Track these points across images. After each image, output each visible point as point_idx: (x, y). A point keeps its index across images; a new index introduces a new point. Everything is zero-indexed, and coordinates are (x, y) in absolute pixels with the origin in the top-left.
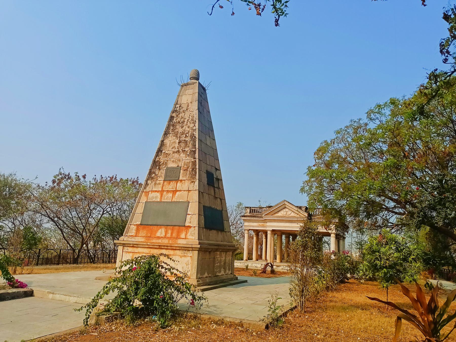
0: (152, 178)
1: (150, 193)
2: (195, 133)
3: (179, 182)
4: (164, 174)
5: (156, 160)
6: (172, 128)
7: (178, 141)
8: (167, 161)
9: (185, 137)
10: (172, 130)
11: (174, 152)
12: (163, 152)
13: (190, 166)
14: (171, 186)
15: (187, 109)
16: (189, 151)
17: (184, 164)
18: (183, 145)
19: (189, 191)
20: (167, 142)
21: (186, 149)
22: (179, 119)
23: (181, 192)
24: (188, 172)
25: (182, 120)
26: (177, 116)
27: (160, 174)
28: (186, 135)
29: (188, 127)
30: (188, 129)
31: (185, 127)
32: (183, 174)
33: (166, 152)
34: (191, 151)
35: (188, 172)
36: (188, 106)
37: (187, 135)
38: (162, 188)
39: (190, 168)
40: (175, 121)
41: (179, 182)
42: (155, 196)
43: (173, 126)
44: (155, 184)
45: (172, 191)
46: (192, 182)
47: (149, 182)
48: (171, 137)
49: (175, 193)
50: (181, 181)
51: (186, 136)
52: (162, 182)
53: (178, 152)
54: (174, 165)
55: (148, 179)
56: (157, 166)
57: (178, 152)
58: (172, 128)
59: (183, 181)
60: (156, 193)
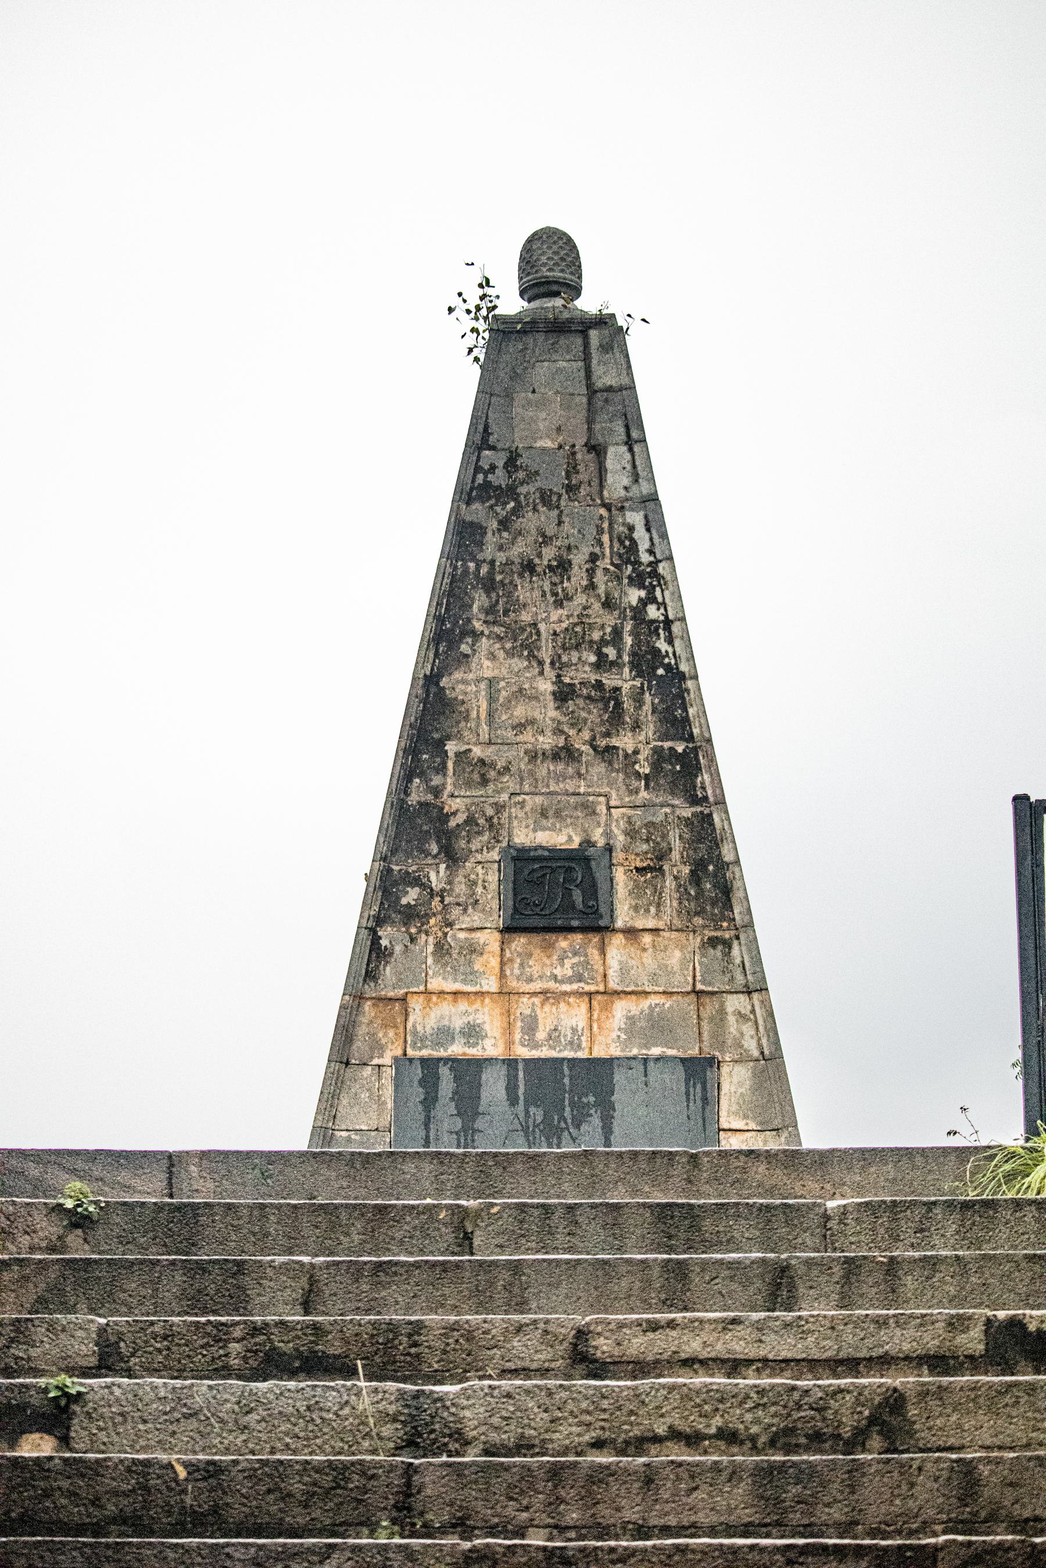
0: (410, 915)
1: (416, 1004)
2: (662, 646)
3: (618, 939)
4: (493, 886)
5: (413, 799)
6: (479, 600)
7: (546, 686)
8: (499, 808)
9: (598, 666)
10: (490, 610)
11: (533, 756)
12: (451, 747)
13: (677, 845)
14: (556, 961)
15: (571, 489)
16: (645, 753)
17: (631, 833)
18: (593, 715)
19: (698, 993)
20: (458, 684)
21: (625, 741)
22: (521, 549)
23: (645, 1004)
24: (669, 883)
25: (549, 553)
26: (504, 524)
27: (460, 888)
28: (600, 655)
29: (608, 604)
30: (610, 620)
31: (581, 599)
32: (636, 891)
33: (477, 752)
34: (659, 758)
35: (669, 883)
36: (572, 469)
37: (611, 652)
38: (502, 975)
39: (675, 855)
40: (501, 557)
41: (618, 939)
42: (458, 1023)
43: (489, 585)
44: (441, 949)
45: (579, 994)
46: (713, 942)
47: (387, 935)
48: (492, 656)
49: (606, 1008)
50: (631, 933)
51: (602, 664)
52: (490, 939)
53: (566, 753)
54: (561, 837)
55: (380, 921)
56: (425, 837)
57: (566, 753)
58: (479, 600)
59: (647, 939)
60: (463, 1005)
